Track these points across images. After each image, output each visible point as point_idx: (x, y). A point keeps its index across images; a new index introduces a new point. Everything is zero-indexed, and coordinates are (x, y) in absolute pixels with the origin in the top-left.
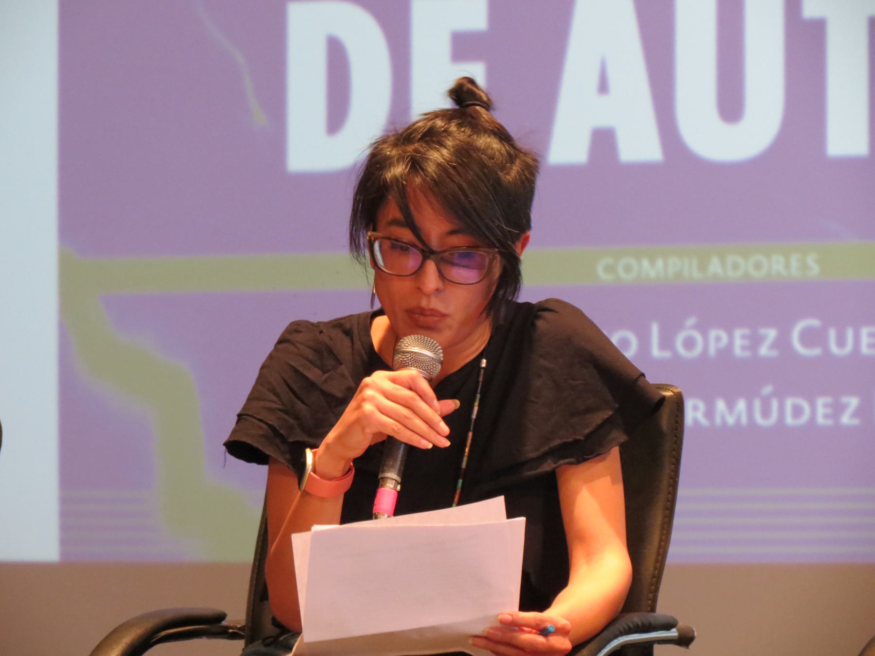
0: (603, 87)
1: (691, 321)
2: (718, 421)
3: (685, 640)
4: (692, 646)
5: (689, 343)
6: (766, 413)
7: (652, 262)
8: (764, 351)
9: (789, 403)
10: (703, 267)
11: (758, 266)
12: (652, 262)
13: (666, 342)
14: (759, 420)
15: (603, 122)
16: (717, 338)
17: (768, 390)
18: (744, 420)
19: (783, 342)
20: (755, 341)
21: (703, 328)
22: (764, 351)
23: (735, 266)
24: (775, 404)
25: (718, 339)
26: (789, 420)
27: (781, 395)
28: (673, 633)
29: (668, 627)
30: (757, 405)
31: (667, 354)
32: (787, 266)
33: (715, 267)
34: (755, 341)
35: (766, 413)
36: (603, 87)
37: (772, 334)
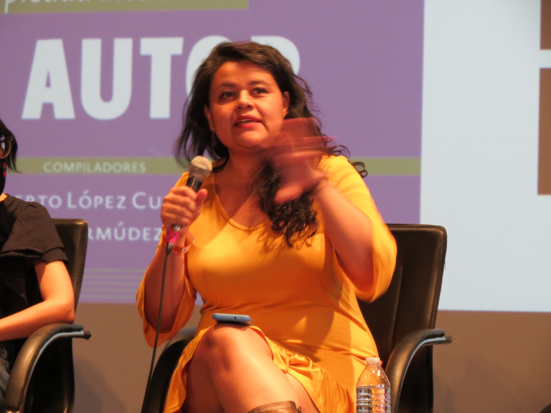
0: (48, 84)
1: (86, 192)
2: (98, 237)
3: (87, 336)
4: (91, 339)
5: (85, 202)
6: (120, 234)
7: (69, 164)
8: (120, 206)
9: (131, 230)
10: (92, 167)
11: (117, 167)
12: (69, 164)
13: (75, 201)
14: (117, 237)
15: (48, 100)
16: (98, 200)
17: (121, 224)
18: (110, 237)
19: (128, 203)
20: (115, 202)
21: (92, 195)
22: (120, 206)
23: (107, 167)
24: (124, 231)
25: (98, 200)
26: (130, 238)
27: (127, 226)
28: (82, 333)
29: (79, 330)
30: (116, 231)
31: (75, 207)
32: (131, 168)
33: (98, 167)
34: (115, 202)
35: (120, 234)
36: (48, 84)
37: (123, 198)
